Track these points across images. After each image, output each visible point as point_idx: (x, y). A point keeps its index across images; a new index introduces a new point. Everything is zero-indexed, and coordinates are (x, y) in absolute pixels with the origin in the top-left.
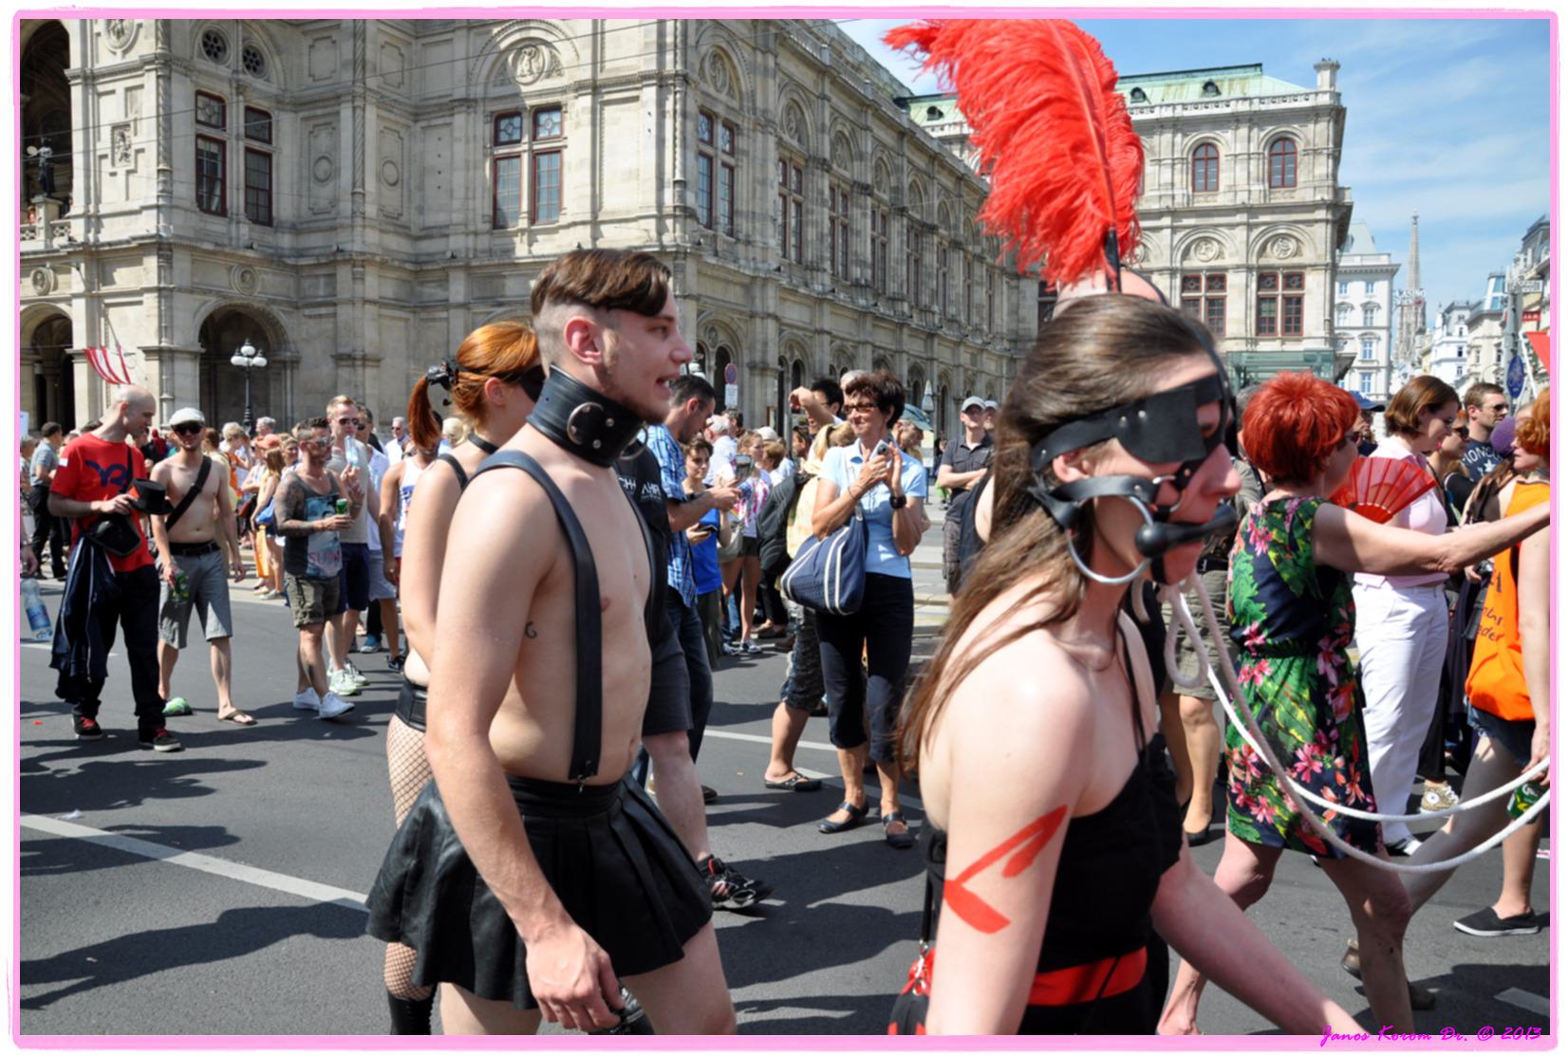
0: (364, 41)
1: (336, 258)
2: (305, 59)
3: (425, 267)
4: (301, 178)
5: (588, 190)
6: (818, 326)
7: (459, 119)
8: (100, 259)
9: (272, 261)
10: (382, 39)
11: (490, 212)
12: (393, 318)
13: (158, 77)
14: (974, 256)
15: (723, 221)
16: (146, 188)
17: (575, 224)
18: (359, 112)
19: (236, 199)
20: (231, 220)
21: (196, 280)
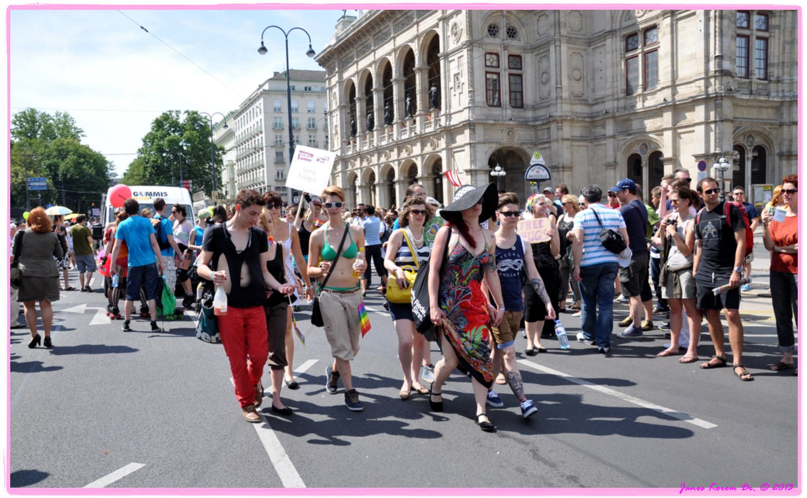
1: (550, 120)
2: (536, 25)
3: (596, 119)
4: (536, 83)
5: (669, 69)
7: (608, 42)
8: (451, 132)
9: (522, 125)
11: (624, 87)
12: (580, 146)
13: (468, 50)
15: (758, 73)
16: (465, 100)
17: (663, 88)
18: (558, 48)
19: (505, 98)
20: (503, 108)
21: (486, 137)
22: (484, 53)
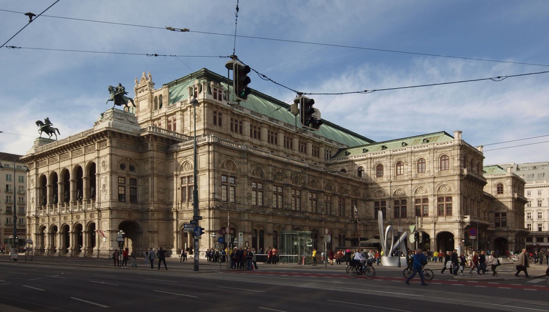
0: (153, 163)
6: (268, 222)
10: (158, 162)
14: (346, 197)
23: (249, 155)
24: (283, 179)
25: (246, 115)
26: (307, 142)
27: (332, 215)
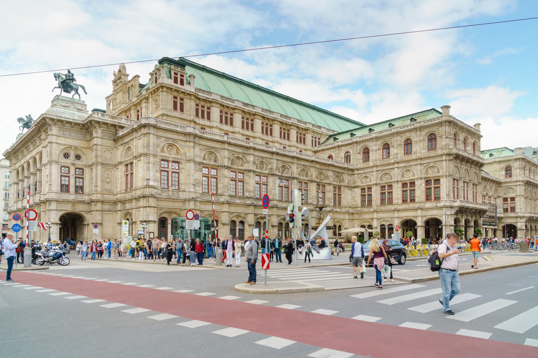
7: (120, 166)
10: (104, 150)
14: (326, 183)
22: (60, 166)
23: (197, 139)
24: (244, 165)
25: (213, 101)
26: (290, 129)
27: (309, 203)
